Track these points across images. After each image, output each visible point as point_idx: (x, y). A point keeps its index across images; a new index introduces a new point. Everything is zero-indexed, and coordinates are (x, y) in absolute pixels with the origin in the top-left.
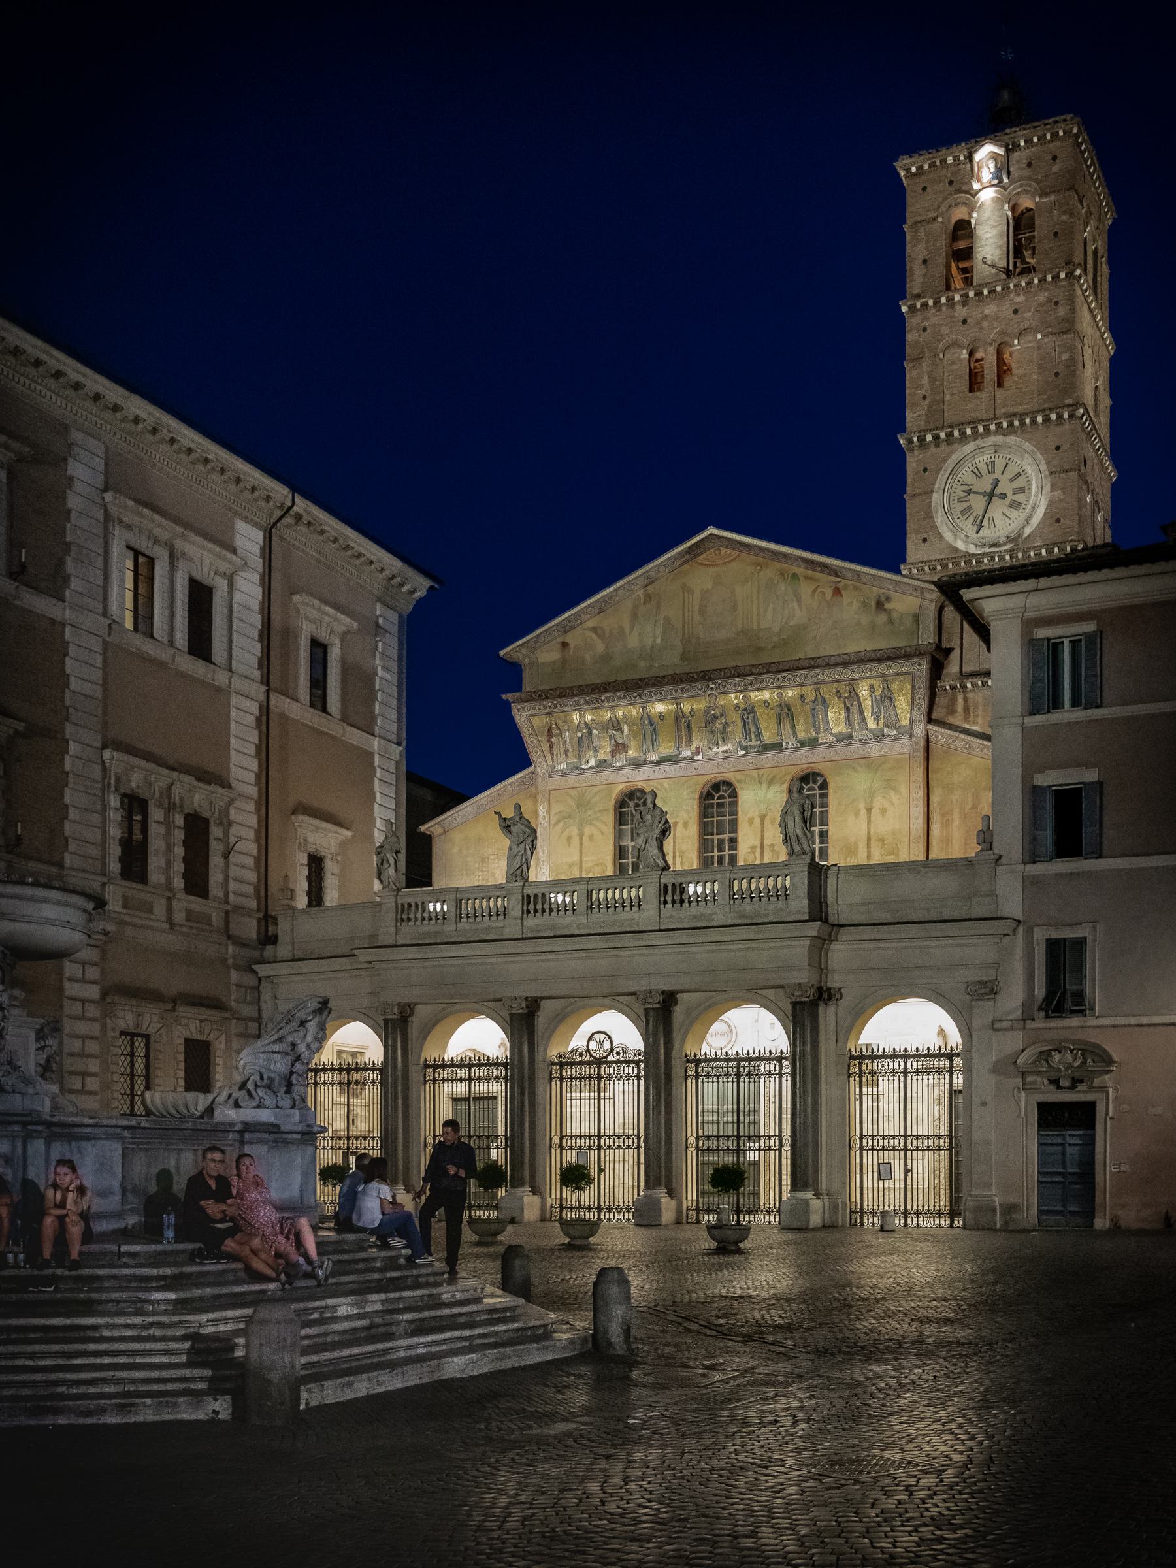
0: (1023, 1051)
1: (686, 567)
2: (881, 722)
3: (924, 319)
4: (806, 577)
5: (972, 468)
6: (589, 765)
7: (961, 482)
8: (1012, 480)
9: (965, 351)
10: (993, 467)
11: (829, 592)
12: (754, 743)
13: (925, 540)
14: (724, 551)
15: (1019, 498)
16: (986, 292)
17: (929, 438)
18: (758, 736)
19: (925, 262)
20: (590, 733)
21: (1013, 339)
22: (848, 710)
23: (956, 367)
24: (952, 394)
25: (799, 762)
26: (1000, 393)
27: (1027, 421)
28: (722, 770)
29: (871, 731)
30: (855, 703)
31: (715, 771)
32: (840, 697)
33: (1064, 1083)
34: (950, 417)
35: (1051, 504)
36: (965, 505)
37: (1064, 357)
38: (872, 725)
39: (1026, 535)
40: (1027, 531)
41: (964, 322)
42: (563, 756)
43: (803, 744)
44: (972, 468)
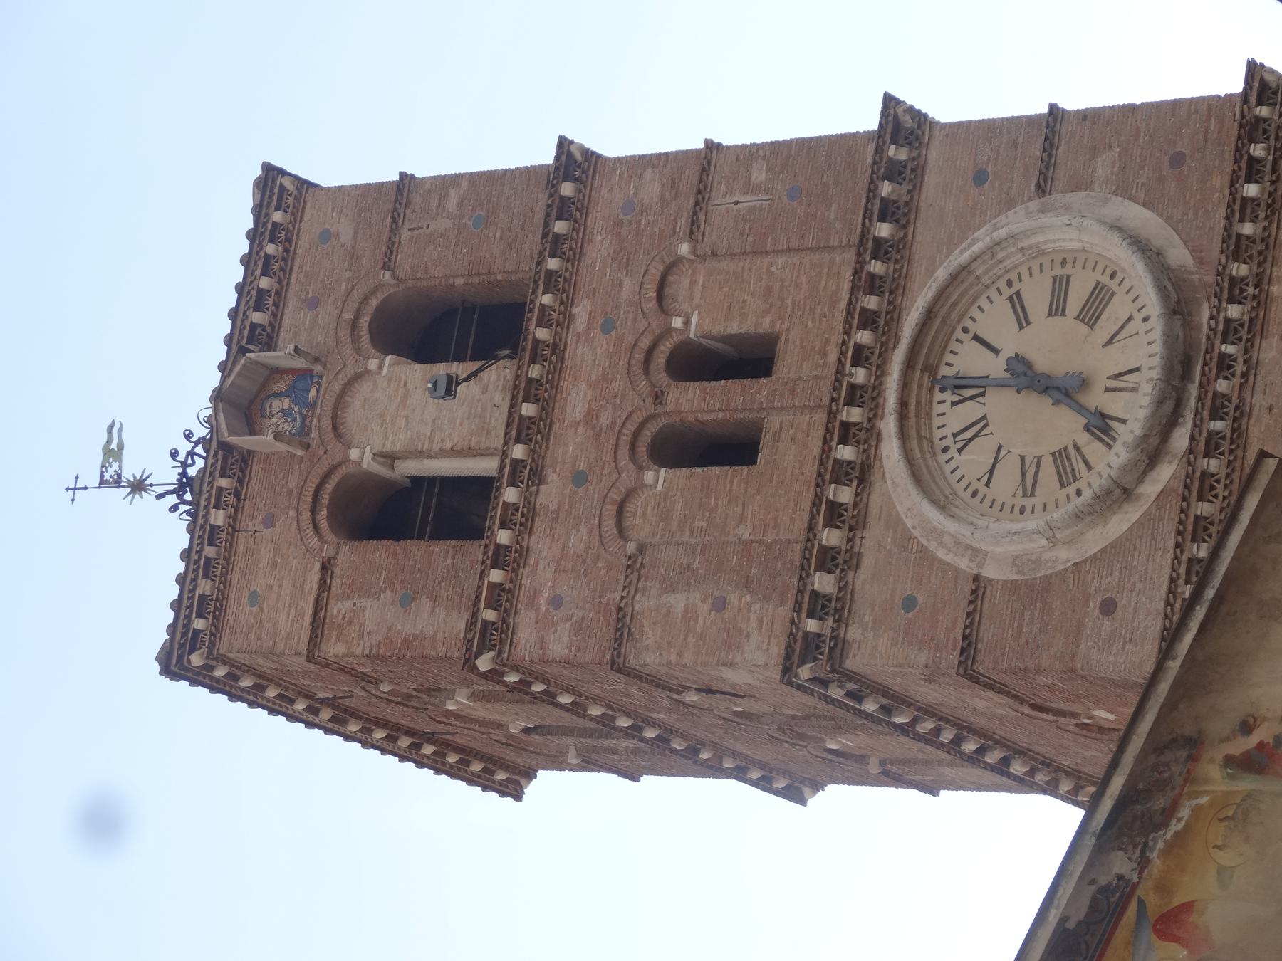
3: (532, 604)
5: (953, 452)
7: (980, 486)
8: (1023, 321)
9: (649, 477)
15: (1075, 303)
16: (528, 409)
17: (823, 582)
19: (406, 602)
21: (669, 331)
23: (678, 506)
24: (741, 520)
26: (786, 366)
27: (876, 267)
35: (1123, 190)
36: (1048, 468)
37: (759, 175)
41: (579, 479)
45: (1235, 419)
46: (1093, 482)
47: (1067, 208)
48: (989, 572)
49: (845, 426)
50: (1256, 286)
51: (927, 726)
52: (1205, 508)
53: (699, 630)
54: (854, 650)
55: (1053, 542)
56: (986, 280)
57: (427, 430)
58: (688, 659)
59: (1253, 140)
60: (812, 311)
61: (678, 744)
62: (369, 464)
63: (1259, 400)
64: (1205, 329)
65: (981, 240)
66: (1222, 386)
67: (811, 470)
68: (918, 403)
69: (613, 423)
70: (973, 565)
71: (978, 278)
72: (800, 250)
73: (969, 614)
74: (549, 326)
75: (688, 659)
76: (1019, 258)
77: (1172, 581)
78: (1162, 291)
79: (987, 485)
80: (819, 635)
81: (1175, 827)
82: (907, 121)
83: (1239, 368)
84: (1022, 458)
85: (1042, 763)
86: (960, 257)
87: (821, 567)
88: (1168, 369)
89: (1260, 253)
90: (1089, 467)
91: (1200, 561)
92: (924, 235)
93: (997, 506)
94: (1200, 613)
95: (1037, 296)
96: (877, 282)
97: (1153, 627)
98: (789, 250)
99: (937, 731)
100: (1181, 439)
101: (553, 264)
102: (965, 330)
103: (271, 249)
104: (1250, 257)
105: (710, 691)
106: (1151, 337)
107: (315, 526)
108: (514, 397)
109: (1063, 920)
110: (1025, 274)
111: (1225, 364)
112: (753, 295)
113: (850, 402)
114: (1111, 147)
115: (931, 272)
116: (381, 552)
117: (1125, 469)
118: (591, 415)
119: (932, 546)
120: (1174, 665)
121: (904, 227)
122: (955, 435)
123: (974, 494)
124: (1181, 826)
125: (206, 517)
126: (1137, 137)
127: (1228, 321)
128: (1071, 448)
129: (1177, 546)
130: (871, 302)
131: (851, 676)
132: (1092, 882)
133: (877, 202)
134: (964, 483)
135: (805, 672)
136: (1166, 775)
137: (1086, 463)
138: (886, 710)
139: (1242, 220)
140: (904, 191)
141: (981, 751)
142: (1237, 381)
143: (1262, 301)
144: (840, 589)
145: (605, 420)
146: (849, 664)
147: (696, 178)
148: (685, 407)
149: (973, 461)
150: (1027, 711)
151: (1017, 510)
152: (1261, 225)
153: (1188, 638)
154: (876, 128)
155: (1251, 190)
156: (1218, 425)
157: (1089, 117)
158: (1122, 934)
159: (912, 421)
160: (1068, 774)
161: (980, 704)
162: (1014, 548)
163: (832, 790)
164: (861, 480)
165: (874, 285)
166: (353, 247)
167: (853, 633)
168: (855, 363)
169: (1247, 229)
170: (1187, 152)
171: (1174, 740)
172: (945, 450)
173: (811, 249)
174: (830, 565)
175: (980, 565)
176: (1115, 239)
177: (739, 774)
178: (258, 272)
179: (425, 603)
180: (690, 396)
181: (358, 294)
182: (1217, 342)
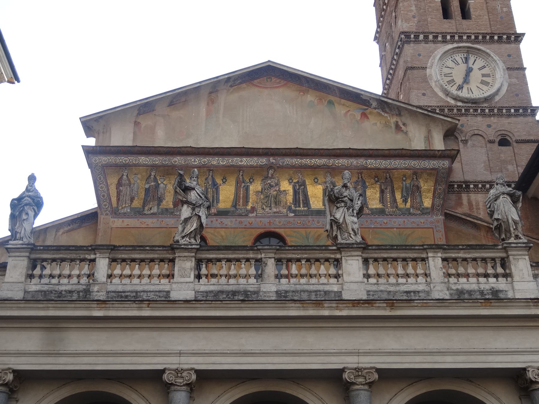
1: (244, 85)
2: (408, 205)
4: (340, 104)
5: (451, 59)
6: (152, 212)
8: (480, 69)
11: (358, 116)
12: (302, 208)
14: (274, 79)
15: (486, 79)
17: (421, 37)
18: (306, 202)
20: (157, 186)
22: (382, 192)
23: (433, 5)
24: (432, 18)
26: (465, 22)
27: (488, 37)
28: (273, 226)
29: (400, 210)
30: (389, 188)
32: (377, 182)
35: (510, 85)
36: (450, 79)
37: (505, 10)
38: (401, 205)
45: (465, 114)
46: (448, 87)
47: (505, 74)
48: (428, 70)
49: (454, 36)
50: (493, 114)
51: (394, 62)
52: (446, 110)
53: (408, 13)
54: (409, 45)
55: (436, 82)
56: (488, 60)
58: (402, 12)
59: (523, 110)
60: (477, 26)
61: (383, 13)
63: (469, 118)
64: (483, 105)
65: (496, 58)
66: (471, 110)
67: (444, 31)
68: (460, 50)
70: (429, 67)
71: (488, 58)
72: (490, 21)
73: (419, 67)
75: (402, 12)
76: (493, 66)
77: (431, 106)
78: (490, 96)
79: (445, 67)
80: (411, 38)
81: (383, 113)
82: (520, 39)
83: (475, 113)
84: (452, 73)
85: (389, 86)
86: (492, 54)
88: (473, 99)
89: (500, 114)
90: (451, 87)
91: (436, 111)
92: (496, 46)
93: (441, 70)
94: (426, 112)
95: (486, 71)
96: (485, 38)
97: (421, 104)
98: (489, 19)
99: (394, 65)
100: (460, 104)
102: (477, 58)
104: (498, 112)
105: (396, 18)
106: (480, 95)
109: (362, 95)
110: (490, 68)
111: (476, 110)
112: (479, 13)
113: (459, 36)
114: (518, 81)
115: (488, 49)
117: (452, 94)
119: (432, 58)
120: (415, 109)
121: (497, 42)
122: (455, 59)
123: (443, 65)
124: (383, 115)
126: (521, 86)
127: (485, 110)
128: (455, 82)
129: (438, 106)
130: (480, 37)
131: (403, 46)
132: (370, 99)
133: (502, 35)
134: (445, 62)
135: (403, 36)
136: (393, 110)
137: (452, 86)
138: (397, 54)
139: (506, 110)
140: (505, 40)
141: (391, 74)
142: (473, 113)
143: (490, 116)
144: (420, 41)
146: (405, 45)
148: (454, 3)
149: (450, 63)
150: (400, 82)
151: (441, 74)
152: (505, 113)
153: (420, 111)
154: (518, 32)
155: (512, 111)
156: (463, 111)
157: (524, 75)
159: (457, 50)
160: (388, 92)
161: (400, 72)
162: (433, 74)
163: (378, 46)
165: (484, 37)
167: (412, 45)
168: (467, 36)
169: (504, 111)
170: (519, 97)
171: (400, 111)
172: (452, 57)
173: (490, 23)
174: (425, 38)
175: (429, 68)
176: (499, 85)
177: (378, 26)
180: (456, 3)
182: (480, 108)
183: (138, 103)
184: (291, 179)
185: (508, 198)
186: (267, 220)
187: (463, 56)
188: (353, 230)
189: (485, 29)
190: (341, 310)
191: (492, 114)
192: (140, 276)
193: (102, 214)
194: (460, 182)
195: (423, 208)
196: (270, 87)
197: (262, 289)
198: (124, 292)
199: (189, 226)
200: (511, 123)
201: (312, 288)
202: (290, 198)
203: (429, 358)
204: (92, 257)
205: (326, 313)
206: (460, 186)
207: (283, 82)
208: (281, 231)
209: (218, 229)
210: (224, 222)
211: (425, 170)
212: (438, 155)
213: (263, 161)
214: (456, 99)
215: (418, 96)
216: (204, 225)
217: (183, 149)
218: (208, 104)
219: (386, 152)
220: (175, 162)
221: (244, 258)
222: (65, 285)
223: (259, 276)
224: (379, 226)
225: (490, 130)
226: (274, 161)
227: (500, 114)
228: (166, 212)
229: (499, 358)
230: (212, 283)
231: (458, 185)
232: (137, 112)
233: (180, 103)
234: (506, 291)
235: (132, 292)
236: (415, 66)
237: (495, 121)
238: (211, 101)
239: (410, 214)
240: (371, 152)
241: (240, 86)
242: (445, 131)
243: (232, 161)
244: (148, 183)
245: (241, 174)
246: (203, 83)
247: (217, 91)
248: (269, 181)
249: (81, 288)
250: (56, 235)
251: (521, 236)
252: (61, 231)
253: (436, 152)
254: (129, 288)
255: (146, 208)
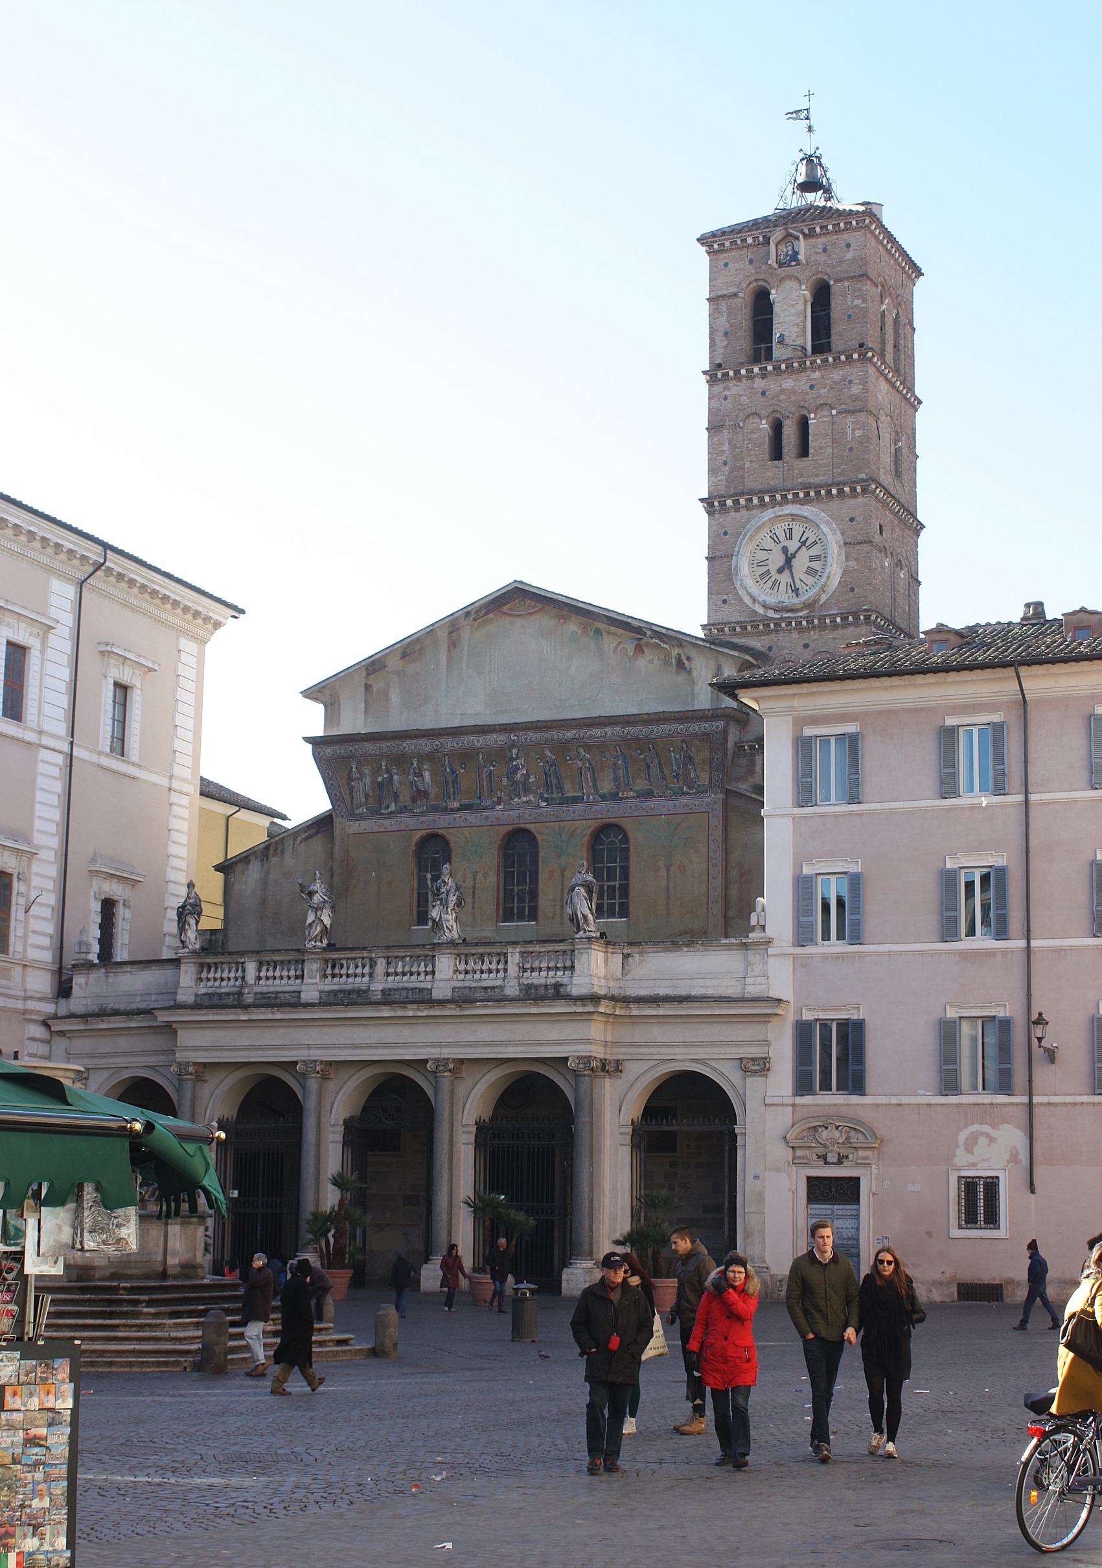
0: (793, 1126)
1: (491, 615)
2: (681, 780)
4: (609, 633)
5: (770, 534)
6: (390, 810)
9: (764, 422)
10: (791, 534)
11: (631, 648)
12: (555, 795)
13: (725, 601)
15: (814, 565)
16: (783, 367)
17: (729, 503)
18: (560, 788)
19: (726, 334)
20: (391, 778)
23: (756, 436)
24: (751, 462)
25: (600, 817)
27: (823, 492)
28: (523, 821)
31: (516, 822)
33: (832, 1158)
34: (751, 483)
35: (845, 573)
36: (764, 569)
37: (858, 433)
39: (821, 602)
40: (824, 598)
41: (763, 393)
42: (363, 800)
43: (603, 797)
44: (770, 534)
48: (734, 558)
52: (749, 628)
57: (781, 320)
60: (814, 468)
62: (771, 297)
69: (780, 401)
72: (833, 458)
74: (811, 364)
83: (789, 628)
87: (734, 501)
92: (835, 504)
98: (833, 453)
100: (771, 614)
101: (831, 359)
103: (842, 225)
107: (750, 284)
108: (786, 360)
110: (822, 544)
116: (744, 317)
118: (783, 391)
119: (741, 537)
125: (749, 236)
130: (812, 494)
142: (785, 628)
143: (808, 630)
145: (782, 397)
147: (858, 408)
153: (701, 643)
155: (838, 620)
156: (772, 626)
158: (634, 635)
164: (761, 505)
166: (844, 261)
167: (717, 516)
172: (771, 531)
178: (833, 223)
179: (725, 343)
181: (828, 270)
183: (363, 664)
184: (539, 758)
185: (582, 890)
186: (516, 813)
187: (787, 527)
188: (447, 927)
189: (827, 472)
190: (422, 1011)
191: (811, 627)
192: (282, 978)
193: (337, 817)
194: (751, 741)
195: (699, 785)
196: (524, 614)
197: (372, 988)
198: (266, 993)
199: (314, 929)
200: (837, 639)
201: (411, 985)
202: (543, 781)
203: (495, 1049)
204: (243, 960)
205: (411, 1014)
206: (752, 747)
207: (539, 606)
208: (531, 827)
209: (461, 829)
210: (468, 818)
211: (695, 736)
212: (710, 715)
213: (502, 738)
214: (765, 606)
215: (716, 605)
216: (328, 927)
217: (410, 732)
218: (449, 647)
219: (645, 716)
220: (404, 748)
221: (359, 958)
222: (225, 988)
223: (371, 975)
224: (645, 814)
225: (807, 650)
226: (515, 738)
227: (822, 626)
228: (403, 810)
229: (549, 1049)
230: (334, 982)
231: (749, 746)
232: (364, 673)
233: (414, 652)
234: (566, 985)
235: (272, 993)
236: (718, 554)
237: (815, 637)
238: (453, 644)
239: (683, 793)
240: (627, 718)
241: (485, 617)
242: (739, 666)
243: (468, 742)
244: (380, 775)
245: (481, 756)
246: (436, 626)
247: (458, 629)
248: (514, 763)
249: (236, 990)
250: (294, 844)
251: (592, 928)
252: (299, 839)
253: (707, 712)
254: (271, 989)
255: (383, 806)
